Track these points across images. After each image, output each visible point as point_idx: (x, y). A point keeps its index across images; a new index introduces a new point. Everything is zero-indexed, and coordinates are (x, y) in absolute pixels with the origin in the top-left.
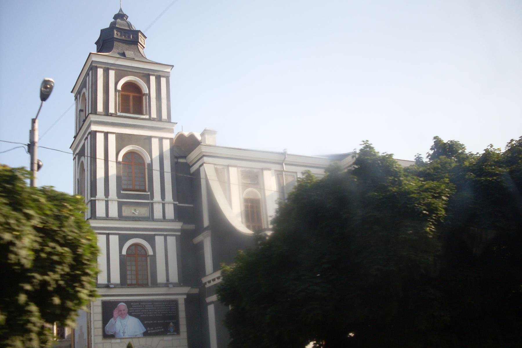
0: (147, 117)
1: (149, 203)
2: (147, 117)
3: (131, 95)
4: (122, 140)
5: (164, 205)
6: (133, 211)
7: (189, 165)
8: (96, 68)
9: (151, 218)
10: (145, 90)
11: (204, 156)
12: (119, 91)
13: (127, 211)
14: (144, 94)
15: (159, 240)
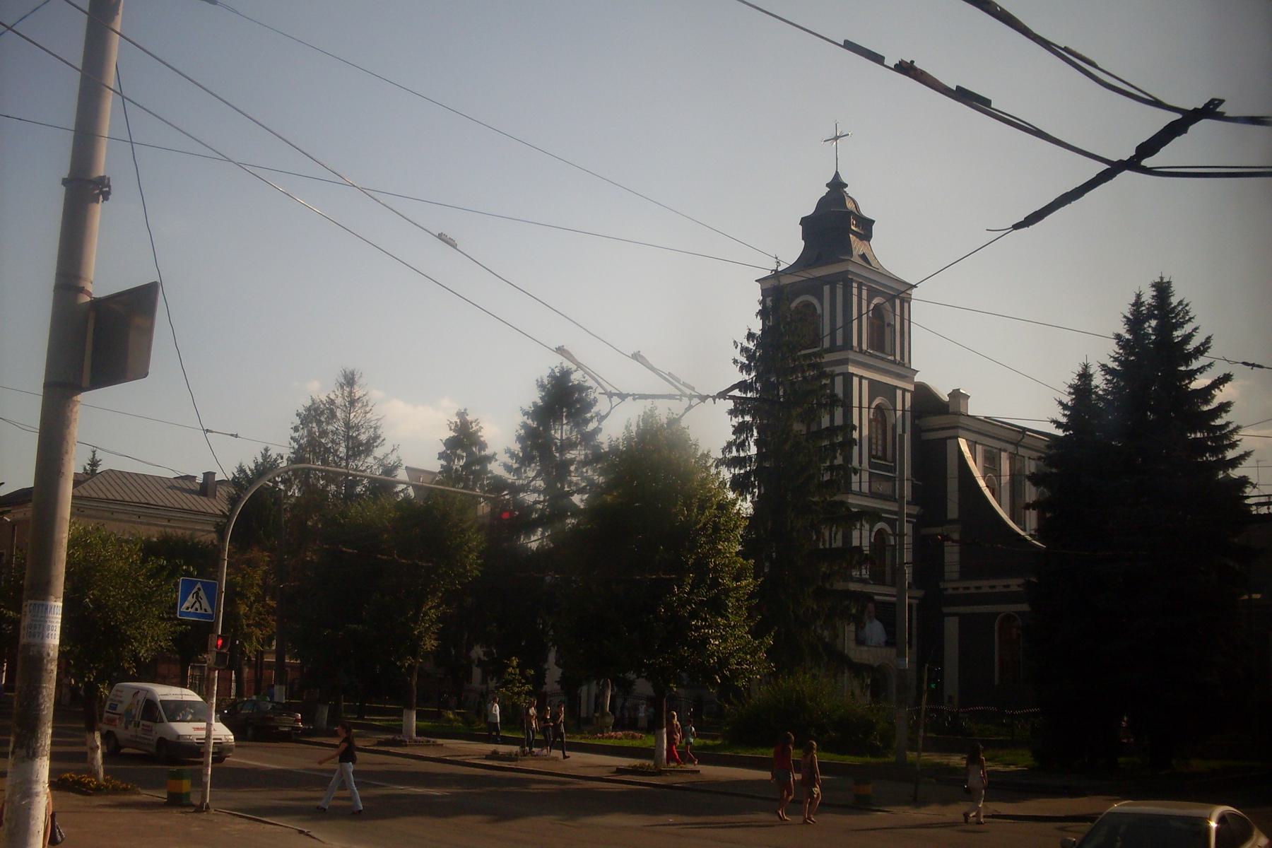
4: (876, 388)
14: (889, 325)
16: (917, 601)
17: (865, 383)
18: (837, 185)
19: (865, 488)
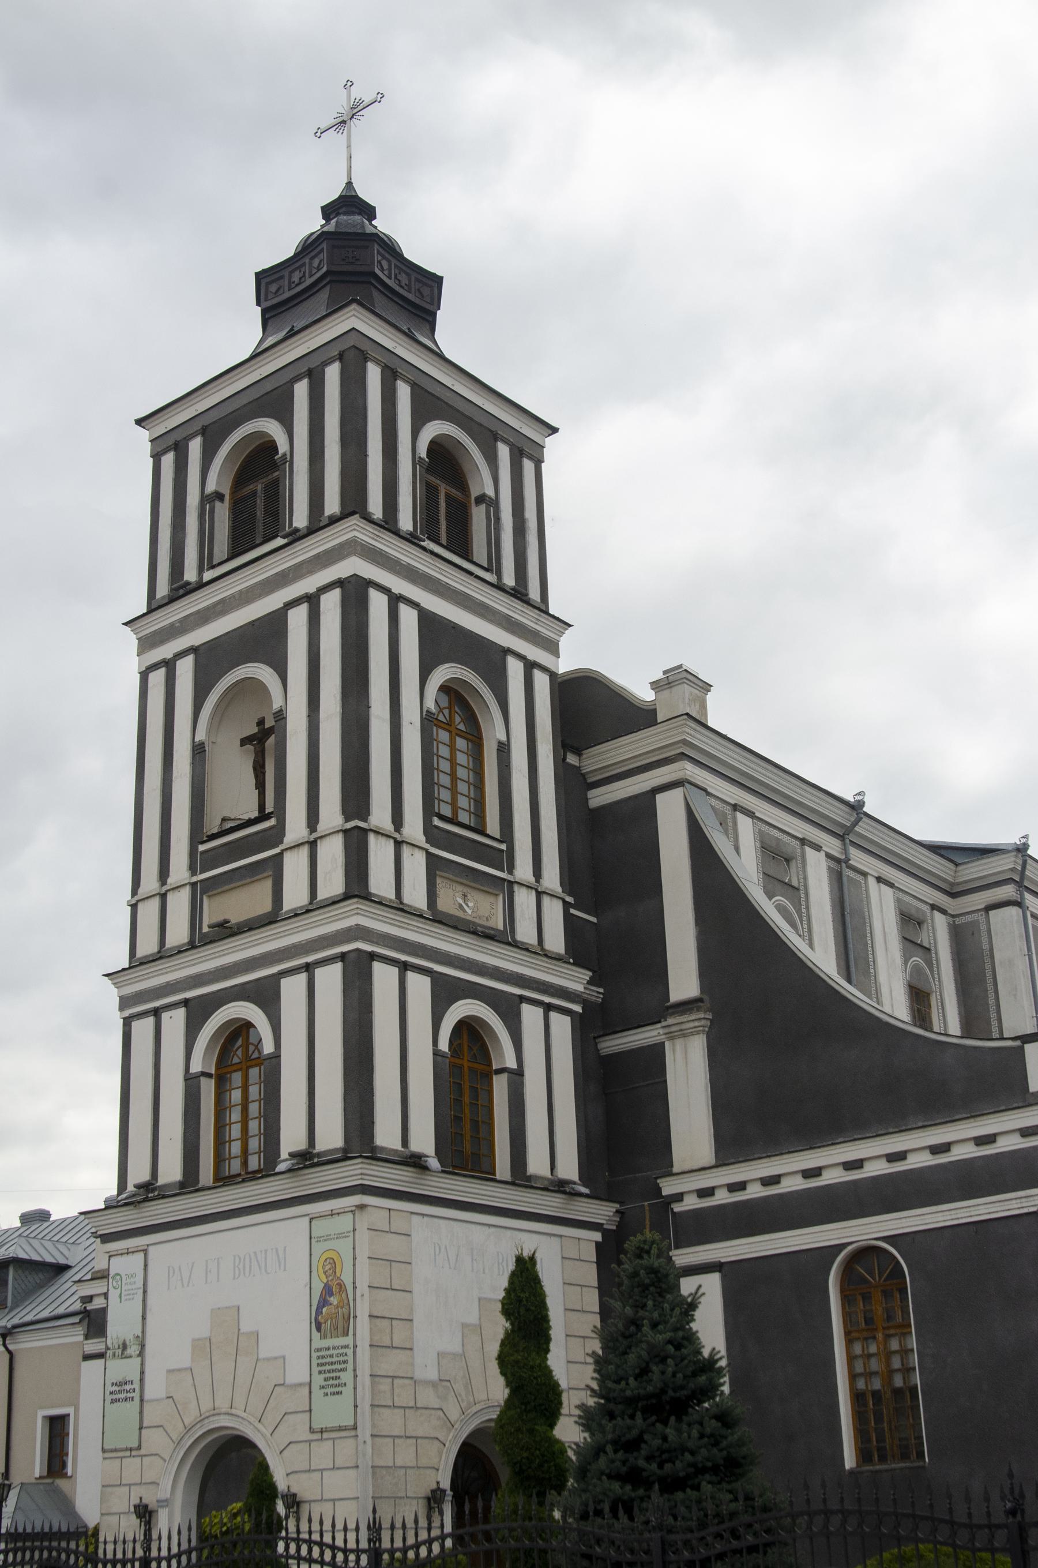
1: (504, 880)
3: (443, 489)
6: (460, 901)
7: (583, 775)
8: (365, 357)
9: (505, 938)
11: (683, 756)
13: (450, 898)
14: (481, 499)
16: (597, 1236)
17: (408, 618)
19: (416, 895)
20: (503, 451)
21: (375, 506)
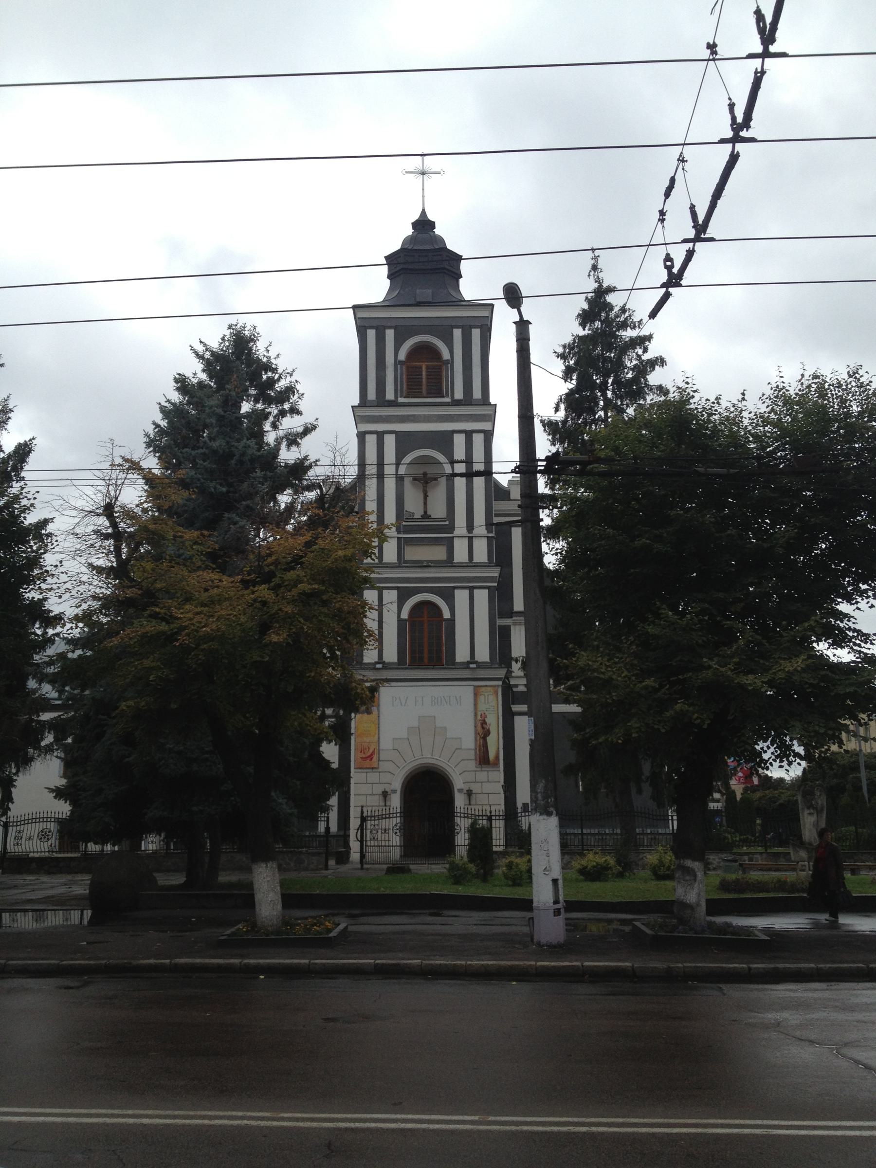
0: (447, 400)
2: (447, 400)
4: (405, 442)
5: (470, 539)
10: (446, 355)
12: (401, 362)
15: (461, 597)
18: (424, 225)
20: (457, 333)
21: (372, 395)
